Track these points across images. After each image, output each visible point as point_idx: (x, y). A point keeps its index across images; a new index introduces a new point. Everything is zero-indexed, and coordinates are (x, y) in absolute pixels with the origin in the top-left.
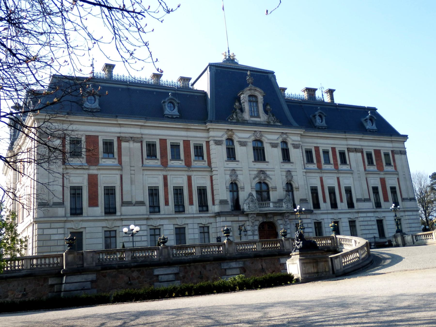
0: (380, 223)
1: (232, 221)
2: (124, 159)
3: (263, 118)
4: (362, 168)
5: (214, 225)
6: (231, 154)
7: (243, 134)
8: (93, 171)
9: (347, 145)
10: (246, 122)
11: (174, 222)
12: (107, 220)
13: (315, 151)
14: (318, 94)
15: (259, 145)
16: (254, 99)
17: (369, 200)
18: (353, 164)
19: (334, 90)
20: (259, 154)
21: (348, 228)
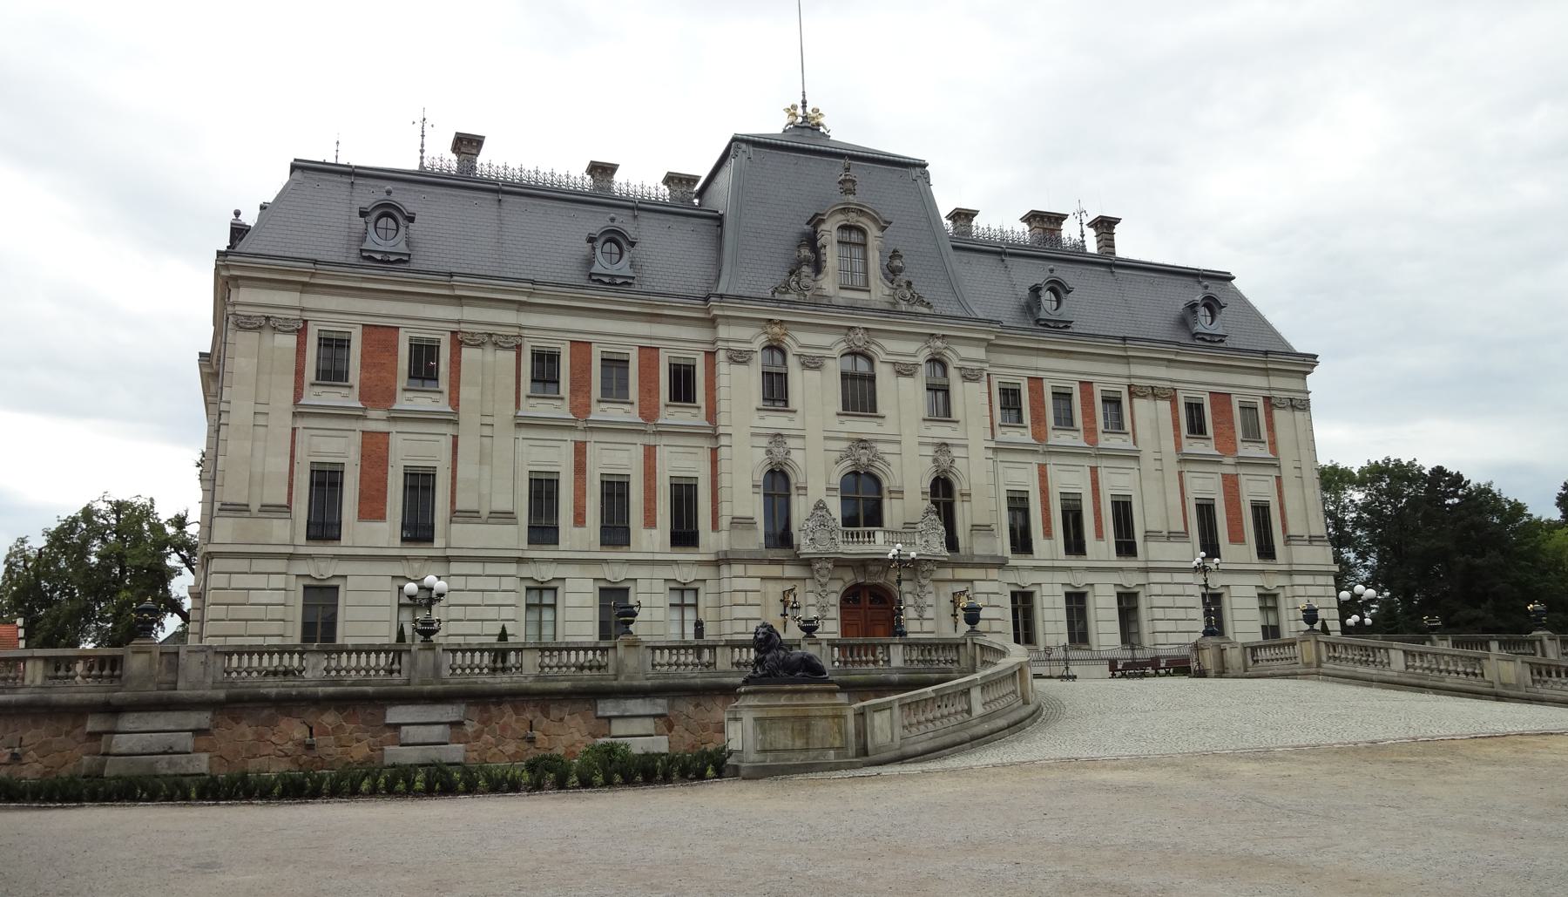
0: (1213, 603)
1: (763, 578)
2: (464, 392)
3: (879, 291)
4: (1169, 445)
5: (711, 586)
6: (776, 390)
8: (376, 422)
9: (1129, 377)
10: (825, 301)
11: (598, 572)
12: (405, 558)
13: (1030, 389)
14: (1070, 231)
15: (862, 366)
16: (855, 237)
17: (1183, 536)
18: (1144, 432)
19: (1117, 221)
20: (859, 395)
21: (1115, 614)
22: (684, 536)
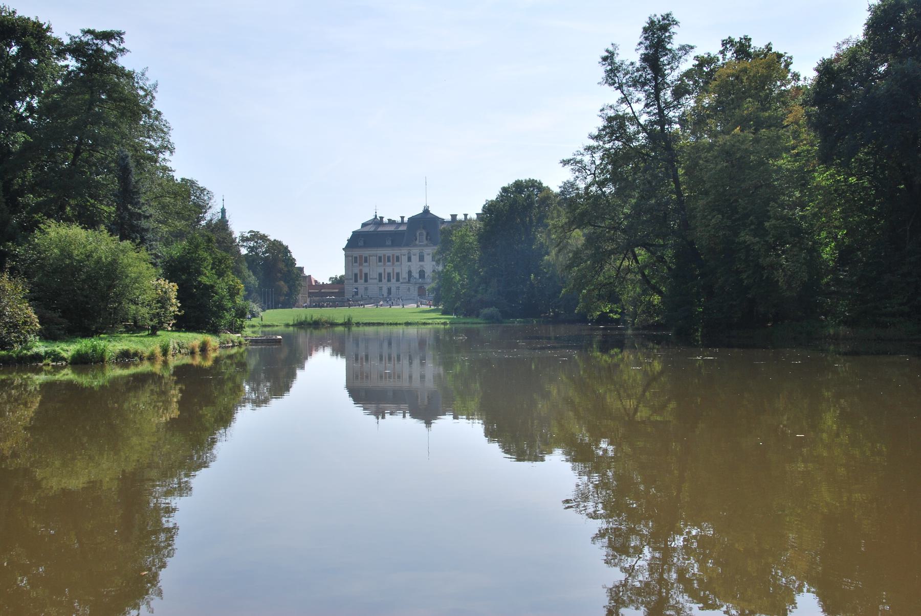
3: (425, 242)
6: (409, 260)
7: (415, 251)
22: (398, 280)
